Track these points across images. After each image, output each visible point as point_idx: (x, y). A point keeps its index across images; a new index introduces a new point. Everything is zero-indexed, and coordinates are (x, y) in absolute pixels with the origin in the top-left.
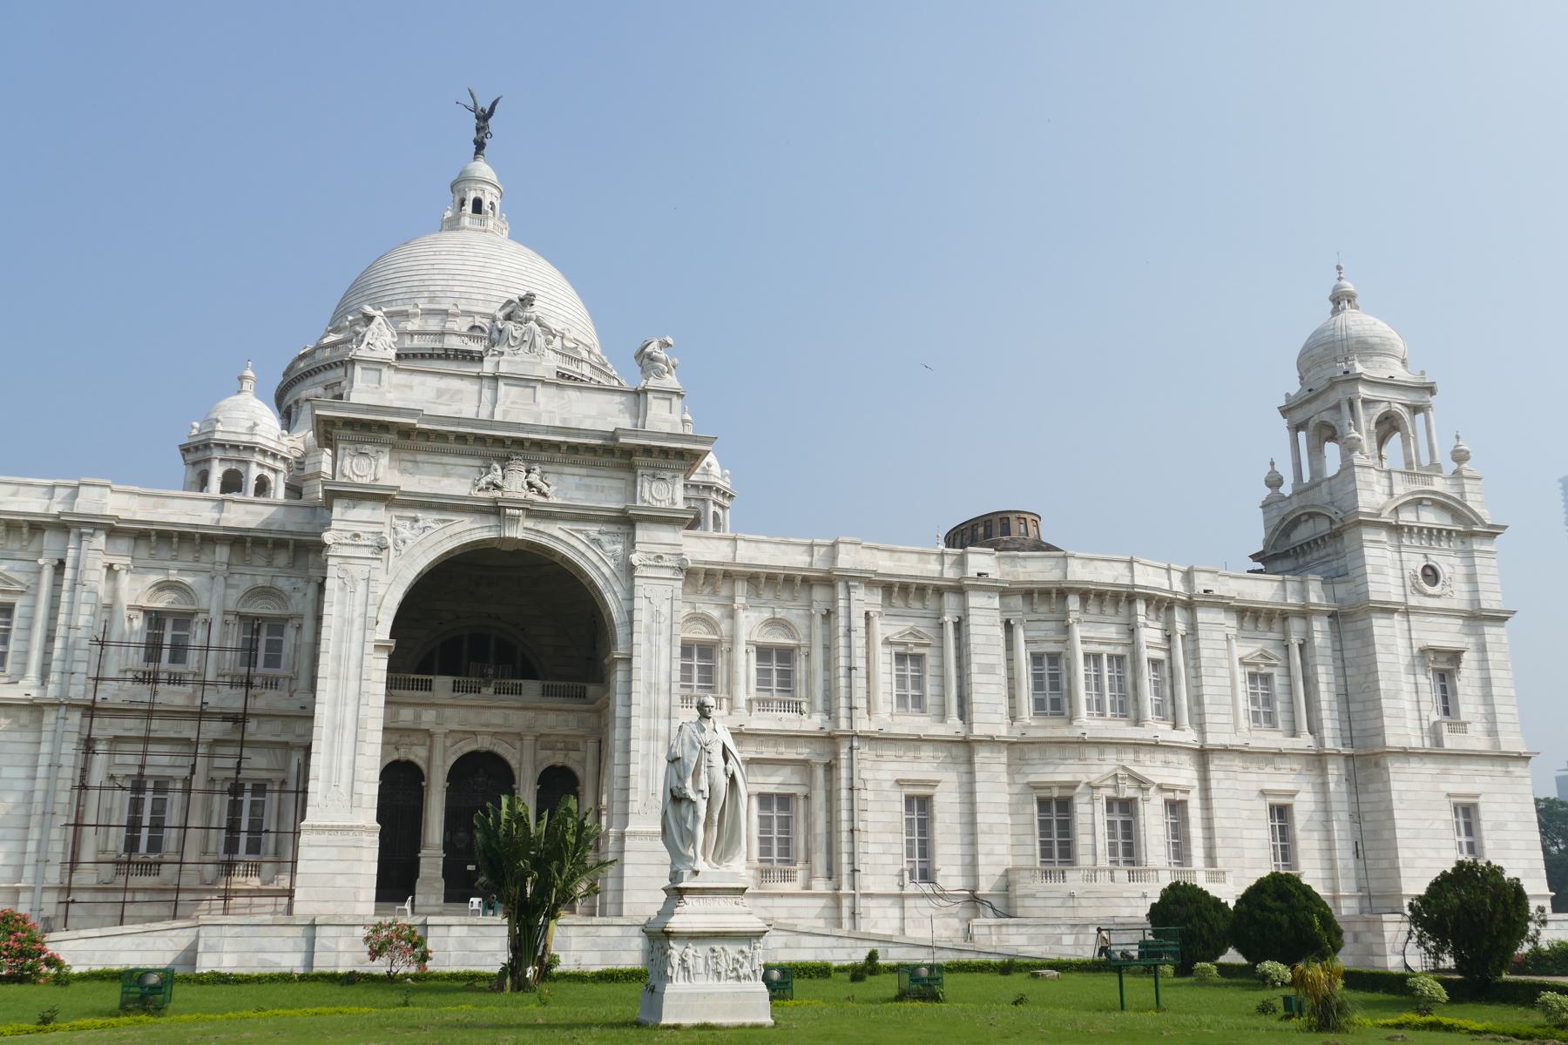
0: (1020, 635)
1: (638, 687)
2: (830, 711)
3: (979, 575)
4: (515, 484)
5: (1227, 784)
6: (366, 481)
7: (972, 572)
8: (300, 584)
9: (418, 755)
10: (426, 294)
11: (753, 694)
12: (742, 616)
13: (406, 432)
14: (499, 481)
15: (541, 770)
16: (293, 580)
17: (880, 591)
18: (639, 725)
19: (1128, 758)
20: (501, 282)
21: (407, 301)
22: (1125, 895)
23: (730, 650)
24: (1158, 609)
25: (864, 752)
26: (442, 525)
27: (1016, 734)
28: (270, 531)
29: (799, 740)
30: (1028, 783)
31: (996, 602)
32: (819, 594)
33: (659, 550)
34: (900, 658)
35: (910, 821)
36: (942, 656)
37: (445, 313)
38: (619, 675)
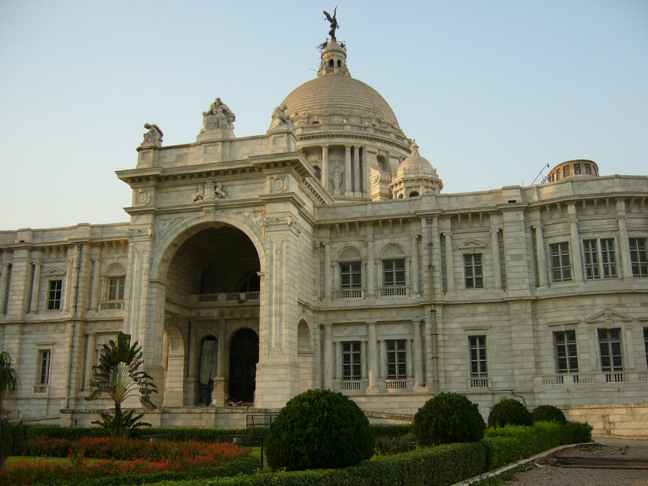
3: (510, 202)
4: (208, 194)
6: (143, 205)
12: (370, 244)
13: (158, 178)
14: (201, 195)
17: (449, 221)
20: (328, 98)
22: (604, 390)
26: (178, 220)
29: (404, 309)
30: (547, 323)
31: (522, 217)
32: (413, 227)
33: (277, 216)
34: (467, 257)
35: (473, 353)
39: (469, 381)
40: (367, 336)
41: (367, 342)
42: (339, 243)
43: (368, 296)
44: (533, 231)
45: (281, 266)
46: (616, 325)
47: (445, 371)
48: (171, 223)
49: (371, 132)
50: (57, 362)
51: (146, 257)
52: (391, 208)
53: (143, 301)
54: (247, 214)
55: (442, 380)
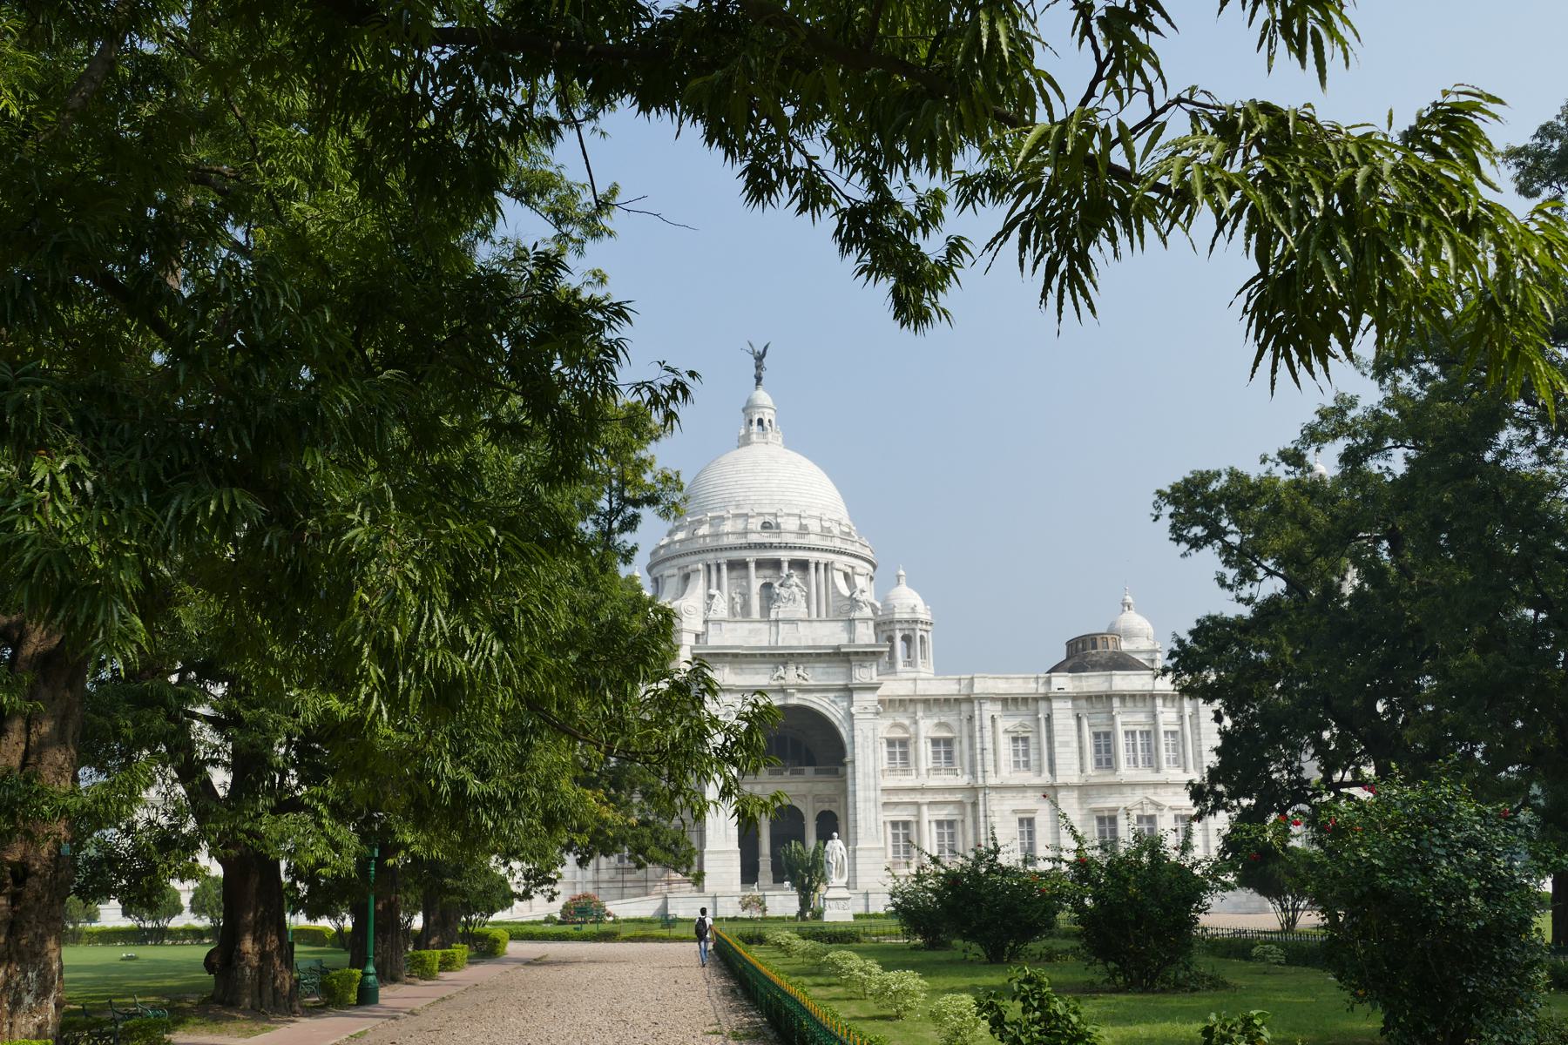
0: (1085, 723)
1: (859, 775)
2: (973, 773)
7: (1054, 688)
11: (930, 765)
12: (921, 723)
18: (860, 794)
19: (1150, 792)
24: (1173, 701)
25: (993, 795)
27: (1083, 781)
32: (965, 707)
33: (866, 704)
34: (1015, 740)
36: (1039, 737)
37: (746, 515)
38: (849, 770)
40: (919, 815)
41: (918, 822)
49: (838, 544)
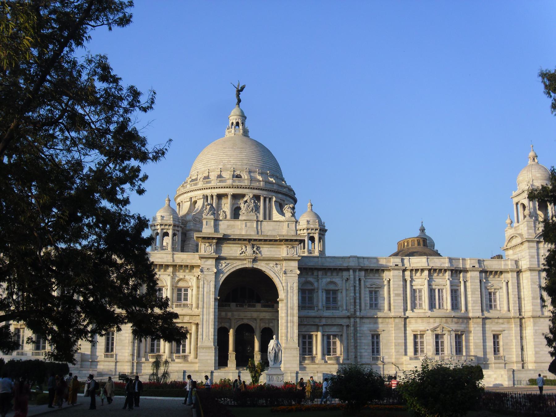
3: (396, 265)
5: (478, 329)
8: (192, 277)
9: (226, 325)
10: (222, 164)
12: (320, 281)
13: (218, 239)
15: (262, 329)
16: (190, 276)
17: (364, 272)
21: (216, 167)
23: (317, 292)
28: (183, 263)
30: (411, 330)
31: (401, 274)
32: (345, 274)
33: (291, 268)
34: (371, 292)
35: (373, 343)
39: (372, 358)
42: (302, 278)
43: (318, 310)
44: (405, 281)
45: (293, 296)
46: (444, 333)
47: (360, 352)
48: (226, 266)
50: (120, 339)
51: (212, 284)
52: (332, 261)
53: (212, 310)
54: (272, 265)
55: (359, 357)
